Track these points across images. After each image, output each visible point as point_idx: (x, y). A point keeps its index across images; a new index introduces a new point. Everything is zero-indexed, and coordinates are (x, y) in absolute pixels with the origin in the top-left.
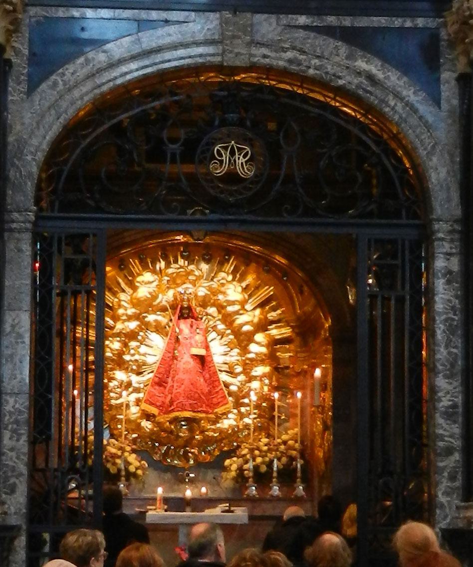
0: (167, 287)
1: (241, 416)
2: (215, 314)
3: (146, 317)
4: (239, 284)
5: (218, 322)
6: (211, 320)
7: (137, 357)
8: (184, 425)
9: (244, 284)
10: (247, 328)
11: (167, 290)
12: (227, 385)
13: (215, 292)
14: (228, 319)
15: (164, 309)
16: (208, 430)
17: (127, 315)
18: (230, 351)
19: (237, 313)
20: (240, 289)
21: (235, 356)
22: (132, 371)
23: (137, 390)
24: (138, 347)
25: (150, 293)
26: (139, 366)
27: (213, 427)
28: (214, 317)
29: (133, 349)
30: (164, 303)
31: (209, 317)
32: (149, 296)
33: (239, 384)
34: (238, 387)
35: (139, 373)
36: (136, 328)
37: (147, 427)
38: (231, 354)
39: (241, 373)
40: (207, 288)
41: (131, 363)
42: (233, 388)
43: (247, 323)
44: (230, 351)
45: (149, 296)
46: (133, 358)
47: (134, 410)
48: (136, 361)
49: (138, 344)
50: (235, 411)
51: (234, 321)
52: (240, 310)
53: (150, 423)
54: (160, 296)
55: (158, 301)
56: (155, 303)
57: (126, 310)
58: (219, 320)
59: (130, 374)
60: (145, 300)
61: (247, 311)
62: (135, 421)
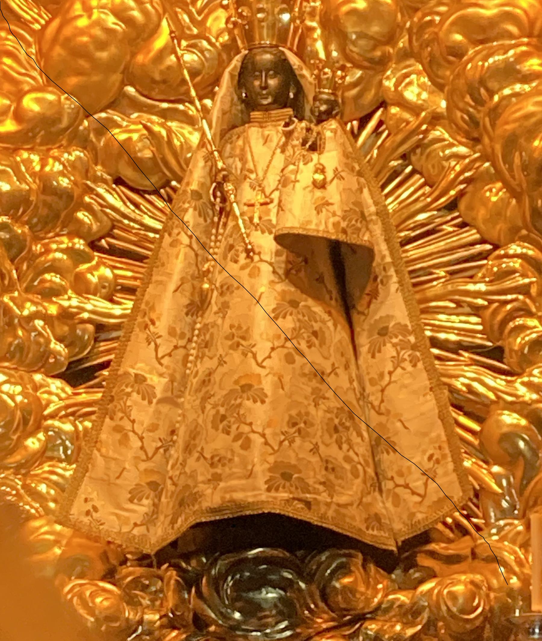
7: (71, 301)
16: (376, 613)
17: (19, 116)
19: (510, 73)
27: (403, 597)
28: (414, 109)
29: (54, 268)
31: (394, 110)
36: (62, 174)
37: (84, 603)
45: (111, 21)
48: (66, 315)
49: (80, 244)
51: (495, 113)
56: (140, 58)
57: (19, 96)
59: (38, 377)
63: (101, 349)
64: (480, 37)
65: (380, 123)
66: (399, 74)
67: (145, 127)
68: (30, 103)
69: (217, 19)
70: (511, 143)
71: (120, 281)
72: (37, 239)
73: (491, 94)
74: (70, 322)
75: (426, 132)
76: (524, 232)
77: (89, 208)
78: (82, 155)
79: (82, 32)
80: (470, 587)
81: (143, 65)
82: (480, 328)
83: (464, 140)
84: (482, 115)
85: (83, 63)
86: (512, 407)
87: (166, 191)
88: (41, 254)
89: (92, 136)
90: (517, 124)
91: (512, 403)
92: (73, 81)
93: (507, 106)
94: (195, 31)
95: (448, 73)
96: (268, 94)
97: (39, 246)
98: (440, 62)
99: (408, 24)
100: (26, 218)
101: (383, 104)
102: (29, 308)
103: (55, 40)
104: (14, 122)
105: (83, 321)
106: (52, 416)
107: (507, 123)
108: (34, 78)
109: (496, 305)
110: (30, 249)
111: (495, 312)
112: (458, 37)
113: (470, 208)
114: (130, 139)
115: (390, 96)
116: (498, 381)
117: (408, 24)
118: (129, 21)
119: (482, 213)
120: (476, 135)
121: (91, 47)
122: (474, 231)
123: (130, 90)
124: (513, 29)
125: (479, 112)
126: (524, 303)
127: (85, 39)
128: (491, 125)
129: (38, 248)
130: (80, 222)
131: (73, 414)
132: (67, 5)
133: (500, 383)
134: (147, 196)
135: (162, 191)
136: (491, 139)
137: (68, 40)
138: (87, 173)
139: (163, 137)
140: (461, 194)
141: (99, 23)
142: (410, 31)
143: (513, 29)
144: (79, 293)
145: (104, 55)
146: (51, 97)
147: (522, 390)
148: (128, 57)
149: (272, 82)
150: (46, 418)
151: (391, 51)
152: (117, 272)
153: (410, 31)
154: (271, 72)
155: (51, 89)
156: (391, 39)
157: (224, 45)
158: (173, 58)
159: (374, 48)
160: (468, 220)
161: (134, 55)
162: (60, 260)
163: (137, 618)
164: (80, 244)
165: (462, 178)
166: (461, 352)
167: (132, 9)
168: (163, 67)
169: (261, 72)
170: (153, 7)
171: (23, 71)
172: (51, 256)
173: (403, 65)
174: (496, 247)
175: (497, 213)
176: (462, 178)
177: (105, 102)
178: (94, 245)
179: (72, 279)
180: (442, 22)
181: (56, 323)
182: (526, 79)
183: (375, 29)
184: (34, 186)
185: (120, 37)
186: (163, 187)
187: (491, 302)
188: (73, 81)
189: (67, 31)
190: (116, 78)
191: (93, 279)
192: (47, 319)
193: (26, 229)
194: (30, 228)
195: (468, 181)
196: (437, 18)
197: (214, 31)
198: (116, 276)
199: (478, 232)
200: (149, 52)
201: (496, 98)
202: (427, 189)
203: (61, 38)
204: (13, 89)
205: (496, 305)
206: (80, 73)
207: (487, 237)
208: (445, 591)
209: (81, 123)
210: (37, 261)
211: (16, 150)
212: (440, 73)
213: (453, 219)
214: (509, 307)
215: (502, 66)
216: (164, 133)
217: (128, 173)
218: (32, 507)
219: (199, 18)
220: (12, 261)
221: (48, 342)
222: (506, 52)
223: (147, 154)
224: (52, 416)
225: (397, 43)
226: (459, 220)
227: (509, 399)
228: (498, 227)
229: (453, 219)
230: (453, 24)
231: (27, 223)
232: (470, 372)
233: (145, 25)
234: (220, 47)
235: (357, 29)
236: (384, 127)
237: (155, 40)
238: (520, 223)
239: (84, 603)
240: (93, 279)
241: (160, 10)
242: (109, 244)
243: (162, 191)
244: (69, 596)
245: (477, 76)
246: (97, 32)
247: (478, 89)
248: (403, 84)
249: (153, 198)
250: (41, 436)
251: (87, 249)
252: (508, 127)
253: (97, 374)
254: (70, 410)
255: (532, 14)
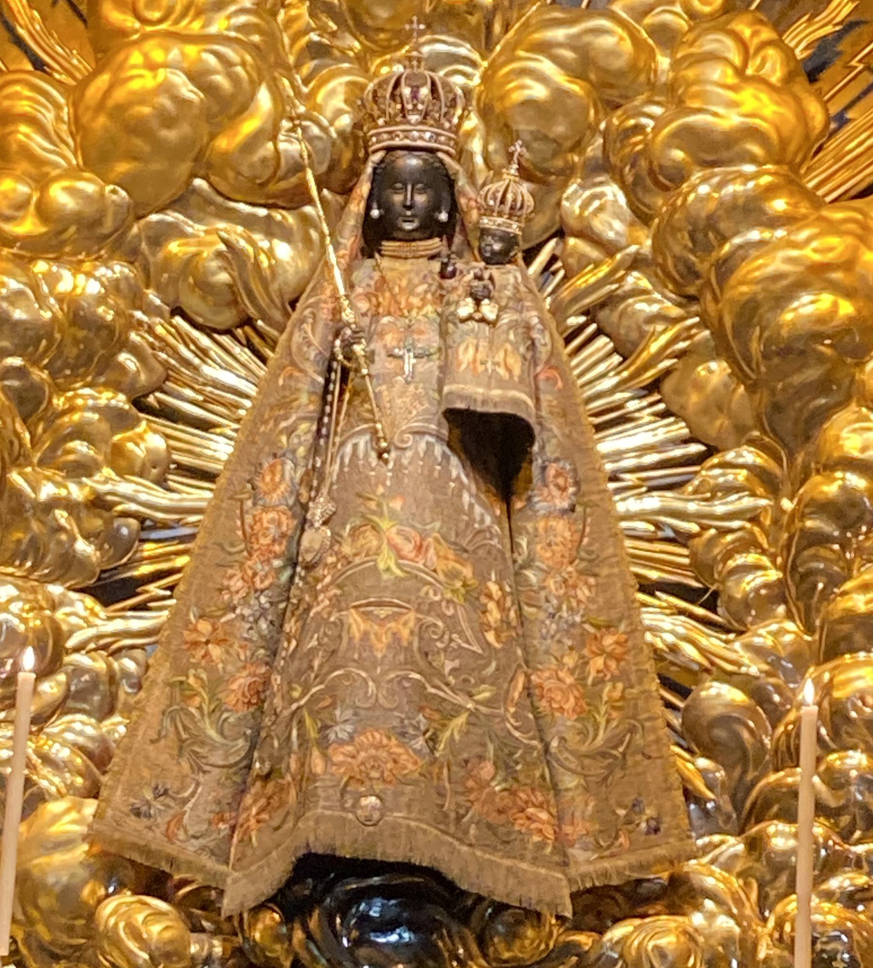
0: (311, 45)
1: (771, 877)
2: (613, 226)
3: (174, 231)
4: (767, 34)
5: (636, 279)
6: (584, 262)
7: (106, 481)
8: (387, 926)
9: (802, 37)
10: (809, 306)
11: (306, 70)
12: (678, 681)
13: (611, 87)
14: (693, 263)
15: (278, 191)
17: (44, 212)
18: (698, 460)
19: (750, 211)
20: (774, 67)
21: (733, 488)
22: (67, 566)
23: (99, 696)
24: (119, 420)
25: (198, 77)
26: (119, 547)
28: (609, 248)
29: (80, 433)
30: (291, 147)
32: (188, 91)
33: (754, 668)
34: (758, 693)
35: (111, 589)
36: (101, 300)
37: (136, 935)
38: (711, 473)
39: (777, 594)
40: (568, 54)
41: (61, 516)
42: (720, 695)
43: (815, 276)
44: (698, 460)
45: (188, 91)
46: (77, 492)
47: (68, 818)
48: (99, 503)
50: (734, 845)
51: (725, 268)
52: (770, 191)
53: (162, 905)
54: (264, 99)
55: (249, 126)
56: (223, 143)
57: (42, 182)
58: (636, 263)
59: (56, 590)
60: (168, 121)
61: (817, 203)
62: (68, 895)
63: (146, 554)
64: (710, 158)
65: (553, 259)
66: (588, 193)
67: (226, 242)
68: (59, 195)
69: (332, 93)
70: (749, 312)
71: (176, 456)
72: (61, 390)
73: (724, 239)
74: (106, 514)
75: (622, 279)
76: (756, 433)
77: (135, 350)
78: (126, 270)
79: (142, 98)
80: (682, 939)
81: (225, 155)
82: (686, 561)
83: (673, 296)
84: (706, 265)
85: (139, 144)
86: (728, 677)
87: (245, 333)
88: (64, 413)
89: (144, 246)
90: (758, 288)
91: (731, 674)
92: (123, 167)
93: (743, 259)
94: (302, 109)
95: (660, 202)
96: (413, 216)
97: (62, 399)
98: (650, 185)
99: (603, 126)
100: (46, 361)
101: (561, 234)
102: (47, 491)
103: (100, 107)
104: (37, 221)
105: (126, 514)
106: (77, 649)
107: (742, 283)
108: (64, 157)
109: (713, 532)
110: (50, 402)
111: (711, 542)
112: (678, 155)
113: (679, 391)
114: (197, 254)
115: (572, 223)
116: (713, 640)
117: (603, 126)
118: (209, 89)
119: (694, 398)
120: (692, 290)
121: (154, 124)
122: (683, 424)
123: (199, 182)
124: (756, 149)
125: (702, 261)
126: (752, 533)
127: (146, 110)
128: (718, 283)
129: (59, 402)
130: (122, 368)
131: (105, 647)
132: (121, 56)
133: (713, 642)
134: (216, 336)
135: (239, 332)
136: (716, 300)
137: (121, 108)
138: (137, 300)
139: (248, 257)
140: (668, 372)
141: (167, 88)
142: (605, 134)
143: (756, 149)
144: (120, 473)
145: (170, 135)
146: (90, 188)
147: (745, 657)
148: (205, 139)
149: (421, 199)
150: (68, 652)
151: (576, 159)
152: (172, 443)
153: (605, 134)
154: (420, 186)
155: (87, 175)
156: (578, 146)
157: (341, 133)
158: (270, 145)
159: (555, 154)
160: (674, 409)
161: (213, 137)
162: (90, 423)
163: (205, 953)
164: (121, 401)
165: (669, 351)
166: (658, 593)
167: (215, 72)
168: (256, 157)
169: (405, 185)
170: (247, 72)
171: (51, 147)
172: (76, 417)
173: (589, 181)
174: (711, 451)
175: (718, 405)
176: (669, 351)
177: (166, 198)
178: (139, 404)
179: (109, 450)
180: (656, 130)
181: (84, 514)
182: (773, 222)
183: (559, 129)
184: (60, 314)
185: (195, 111)
186: (241, 326)
187: (704, 528)
188: (123, 167)
189: (119, 95)
190: (185, 168)
191: (140, 452)
192: (70, 506)
193: (45, 375)
194: (51, 374)
195: (680, 355)
196: (650, 123)
197: (329, 112)
198: (170, 448)
199: (688, 426)
200: (235, 135)
201: (727, 248)
202: (616, 359)
203: (110, 103)
204: (33, 171)
205: (713, 532)
206: (134, 157)
207: (699, 434)
208: (650, 947)
209: (130, 227)
210: (59, 422)
211: (32, 260)
212: (647, 200)
213: (651, 405)
214: (729, 538)
215: (741, 202)
216: (250, 250)
217: (192, 302)
218: (52, 783)
219: (305, 90)
220: (25, 421)
221: (73, 539)
222: (745, 183)
223: (223, 277)
224: (77, 649)
225: (585, 149)
226: (661, 406)
227: (729, 667)
228: (718, 423)
229: (651, 405)
230: (675, 135)
231: (46, 367)
232: (667, 623)
233: (233, 96)
234: (334, 135)
235: (533, 128)
236: (559, 264)
237: (245, 119)
238: (750, 422)
239: (136, 935)
240: (140, 452)
241: (255, 75)
242: (159, 401)
243: (239, 332)
244: (112, 921)
245: (703, 214)
246: (165, 101)
247: (706, 231)
248: (591, 209)
249: (225, 340)
250: (62, 677)
251: (134, 410)
252: (744, 289)
253: (139, 590)
254: (102, 642)
255: (786, 131)
